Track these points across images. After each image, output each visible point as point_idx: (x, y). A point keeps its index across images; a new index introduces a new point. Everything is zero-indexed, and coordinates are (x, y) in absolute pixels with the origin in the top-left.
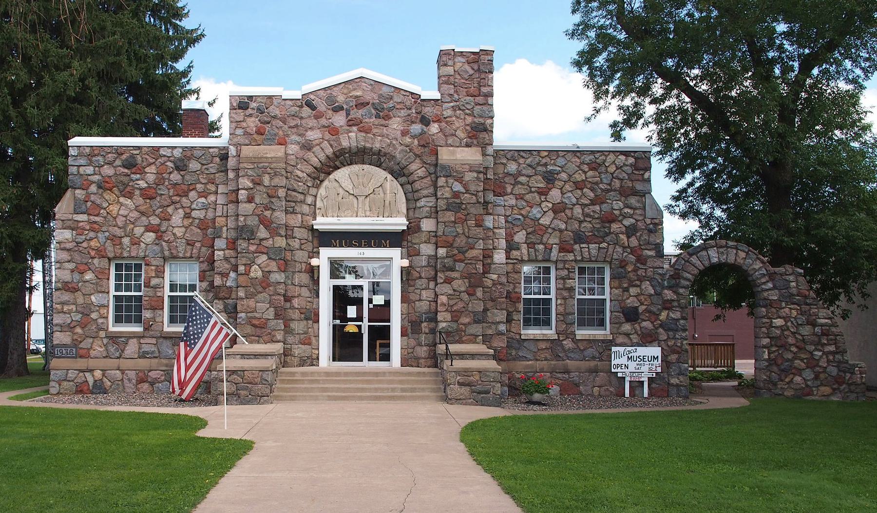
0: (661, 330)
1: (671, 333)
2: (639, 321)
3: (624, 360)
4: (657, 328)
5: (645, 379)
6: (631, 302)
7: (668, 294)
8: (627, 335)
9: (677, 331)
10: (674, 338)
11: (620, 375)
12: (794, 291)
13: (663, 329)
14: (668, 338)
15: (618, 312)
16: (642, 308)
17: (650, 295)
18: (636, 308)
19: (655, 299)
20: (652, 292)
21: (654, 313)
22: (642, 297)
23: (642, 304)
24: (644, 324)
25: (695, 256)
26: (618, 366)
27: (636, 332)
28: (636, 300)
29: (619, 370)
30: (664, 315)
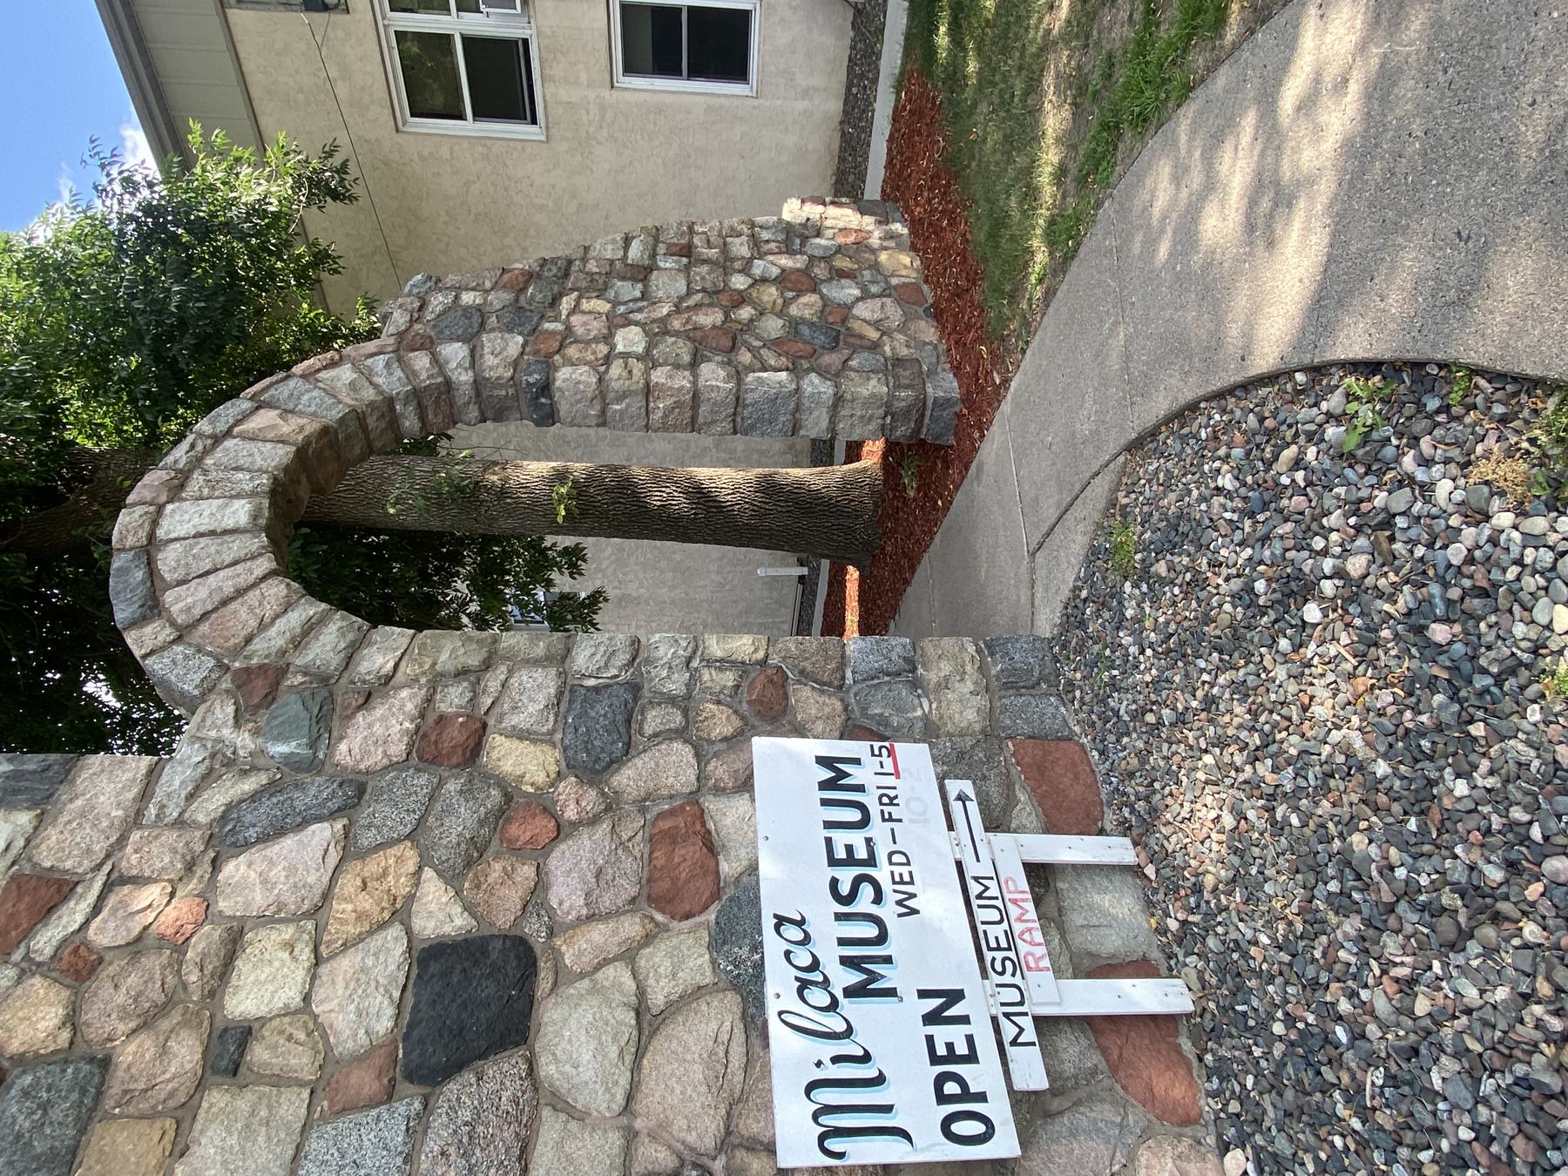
0: (629, 778)
1: (654, 720)
2: (534, 930)
3: (892, 1033)
4: (612, 806)
5: (1013, 851)
6: (363, 1001)
7: (375, 737)
8: (648, 1022)
9: (635, 688)
10: (685, 702)
11: (1031, 1072)
12: (499, 299)
13: (615, 763)
14: (681, 734)
15: (416, 1130)
16: (441, 913)
17: (350, 849)
18: (434, 963)
19: (384, 816)
20: (322, 834)
21: (500, 816)
22: (347, 908)
23: (401, 912)
24: (566, 895)
25: (169, 597)
26: (952, 1093)
27: (629, 955)
28: (346, 964)
29: (983, 1075)
30: (521, 760)
